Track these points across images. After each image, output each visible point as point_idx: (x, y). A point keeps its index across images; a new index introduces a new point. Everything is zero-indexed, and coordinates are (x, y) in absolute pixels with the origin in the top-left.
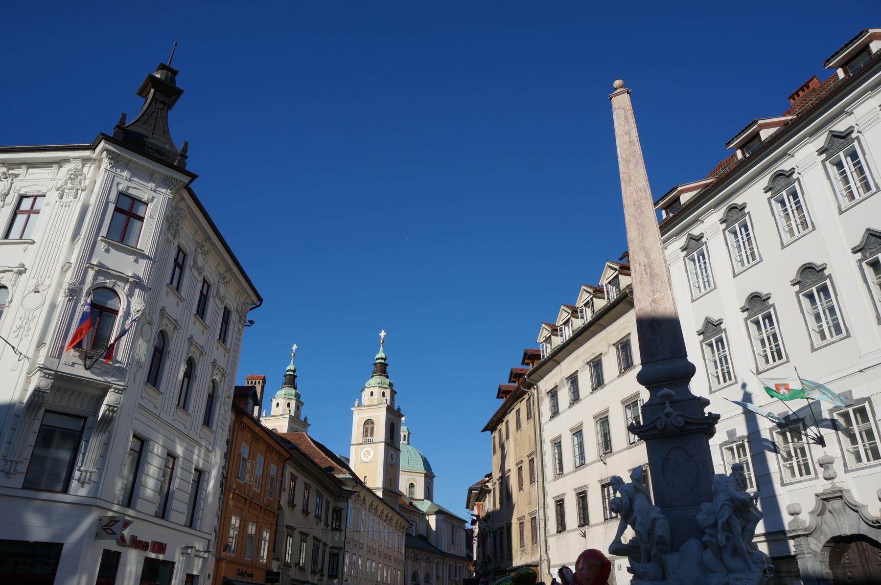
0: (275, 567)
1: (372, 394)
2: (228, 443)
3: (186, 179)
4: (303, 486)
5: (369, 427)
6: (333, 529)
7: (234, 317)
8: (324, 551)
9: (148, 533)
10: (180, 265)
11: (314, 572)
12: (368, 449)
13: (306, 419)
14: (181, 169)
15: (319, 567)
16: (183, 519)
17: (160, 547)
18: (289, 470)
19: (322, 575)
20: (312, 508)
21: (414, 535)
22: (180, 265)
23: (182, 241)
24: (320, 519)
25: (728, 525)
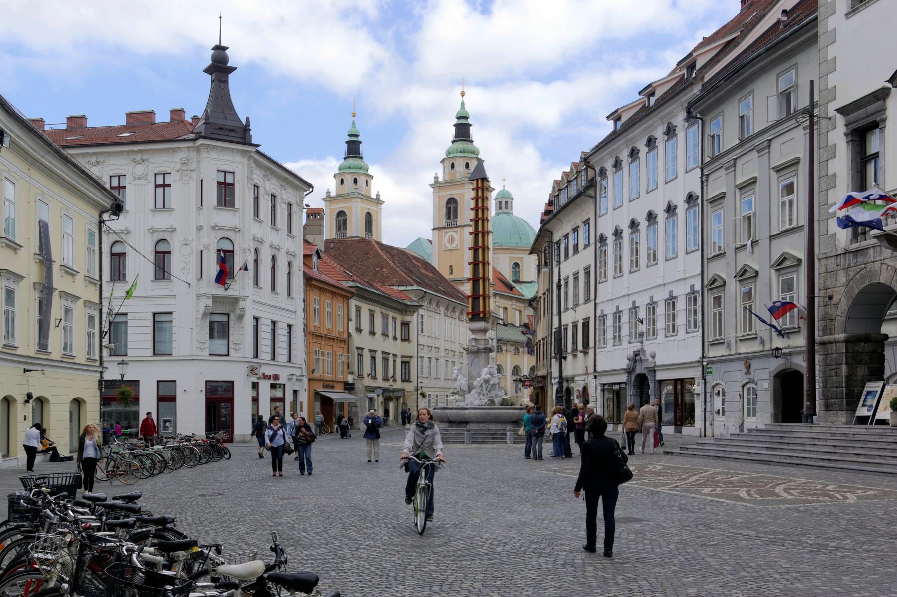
0: (350, 378)
1: (453, 166)
2: (304, 301)
3: (253, 149)
4: (368, 313)
5: (452, 206)
6: (402, 340)
7: (295, 208)
8: (394, 361)
9: (269, 371)
10: (256, 199)
11: (386, 379)
12: (455, 235)
13: (378, 195)
14: (250, 144)
15: (391, 373)
16: (285, 359)
17: (276, 377)
18: (353, 303)
19: (395, 381)
20: (378, 329)
21: (517, 325)
22: (256, 199)
23: (256, 181)
24: (387, 336)
25: (481, 386)
